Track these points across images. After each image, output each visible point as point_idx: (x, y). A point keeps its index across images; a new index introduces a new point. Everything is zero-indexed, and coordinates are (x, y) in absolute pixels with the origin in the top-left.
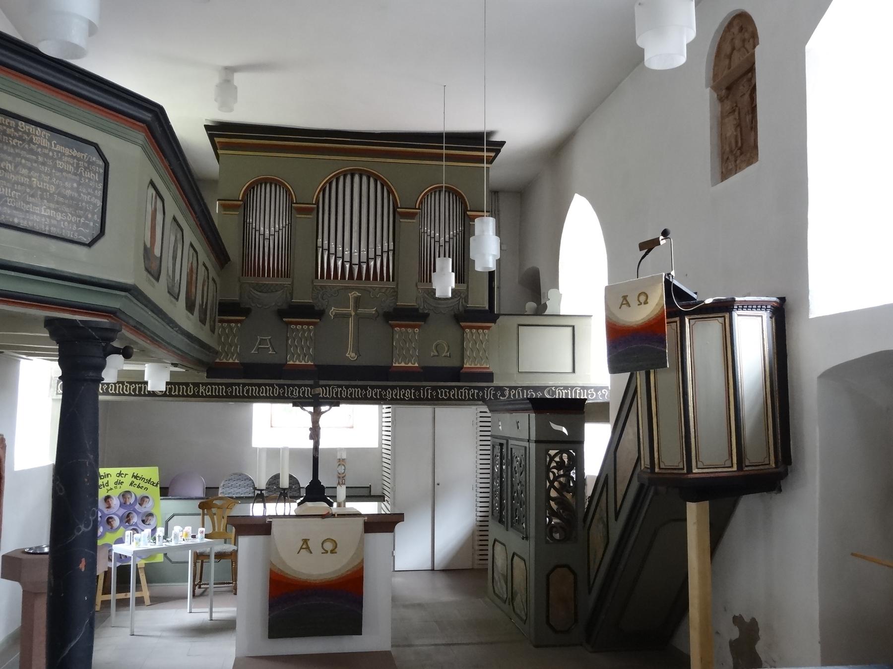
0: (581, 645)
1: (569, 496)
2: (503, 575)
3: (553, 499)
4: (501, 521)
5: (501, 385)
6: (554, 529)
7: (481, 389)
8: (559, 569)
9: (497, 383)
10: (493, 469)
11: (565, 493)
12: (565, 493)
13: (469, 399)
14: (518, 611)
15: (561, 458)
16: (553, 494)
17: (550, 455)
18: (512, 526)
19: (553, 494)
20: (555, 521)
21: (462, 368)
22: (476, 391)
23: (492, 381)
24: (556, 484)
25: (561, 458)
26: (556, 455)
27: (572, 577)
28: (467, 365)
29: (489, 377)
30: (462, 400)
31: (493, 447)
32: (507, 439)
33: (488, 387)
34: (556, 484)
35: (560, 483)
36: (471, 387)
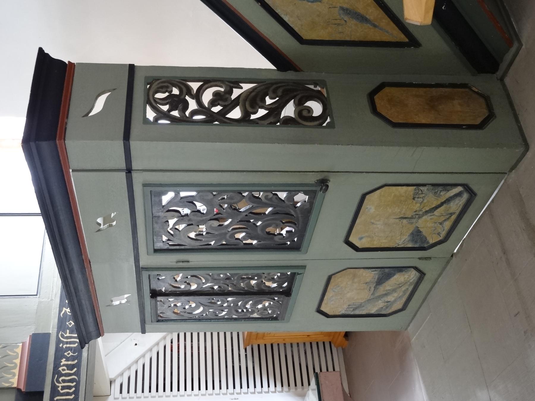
0: (502, 79)
1: (236, 93)
2: (380, 282)
3: (246, 115)
4: (287, 293)
5: (56, 320)
6: (305, 113)
7: (59, 354)
8: (379, 109)
9: (51, 328)
10: (200, 319)
11: (233, 97)
12: (233, 97)
13: (77, 374)
14: (448, 225)
15: (164, 101)
16: (236, 114)
17: (156, 119)
18: (296, 248)
19: (236, 114)
20: (289, 110)
21: (18, 390)
22: (63, 362)
23: (48, 335)
24: (216, 109)
25: (164, 101)
26: (155, 109)
27: (387, 90)
28: (14, 382)
29: (39, 342)
30: (77, 387)
31: (160, 320)
32: (139, 270)
33: (58, 341)
34: (216, 109)
35: (213, 103)
36: (56, 372)
